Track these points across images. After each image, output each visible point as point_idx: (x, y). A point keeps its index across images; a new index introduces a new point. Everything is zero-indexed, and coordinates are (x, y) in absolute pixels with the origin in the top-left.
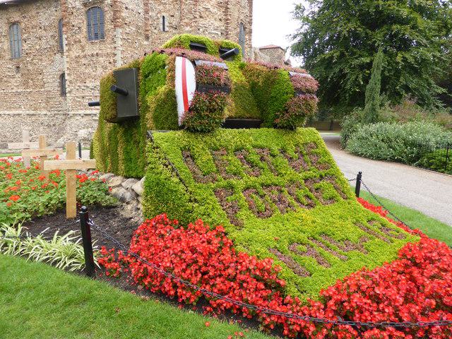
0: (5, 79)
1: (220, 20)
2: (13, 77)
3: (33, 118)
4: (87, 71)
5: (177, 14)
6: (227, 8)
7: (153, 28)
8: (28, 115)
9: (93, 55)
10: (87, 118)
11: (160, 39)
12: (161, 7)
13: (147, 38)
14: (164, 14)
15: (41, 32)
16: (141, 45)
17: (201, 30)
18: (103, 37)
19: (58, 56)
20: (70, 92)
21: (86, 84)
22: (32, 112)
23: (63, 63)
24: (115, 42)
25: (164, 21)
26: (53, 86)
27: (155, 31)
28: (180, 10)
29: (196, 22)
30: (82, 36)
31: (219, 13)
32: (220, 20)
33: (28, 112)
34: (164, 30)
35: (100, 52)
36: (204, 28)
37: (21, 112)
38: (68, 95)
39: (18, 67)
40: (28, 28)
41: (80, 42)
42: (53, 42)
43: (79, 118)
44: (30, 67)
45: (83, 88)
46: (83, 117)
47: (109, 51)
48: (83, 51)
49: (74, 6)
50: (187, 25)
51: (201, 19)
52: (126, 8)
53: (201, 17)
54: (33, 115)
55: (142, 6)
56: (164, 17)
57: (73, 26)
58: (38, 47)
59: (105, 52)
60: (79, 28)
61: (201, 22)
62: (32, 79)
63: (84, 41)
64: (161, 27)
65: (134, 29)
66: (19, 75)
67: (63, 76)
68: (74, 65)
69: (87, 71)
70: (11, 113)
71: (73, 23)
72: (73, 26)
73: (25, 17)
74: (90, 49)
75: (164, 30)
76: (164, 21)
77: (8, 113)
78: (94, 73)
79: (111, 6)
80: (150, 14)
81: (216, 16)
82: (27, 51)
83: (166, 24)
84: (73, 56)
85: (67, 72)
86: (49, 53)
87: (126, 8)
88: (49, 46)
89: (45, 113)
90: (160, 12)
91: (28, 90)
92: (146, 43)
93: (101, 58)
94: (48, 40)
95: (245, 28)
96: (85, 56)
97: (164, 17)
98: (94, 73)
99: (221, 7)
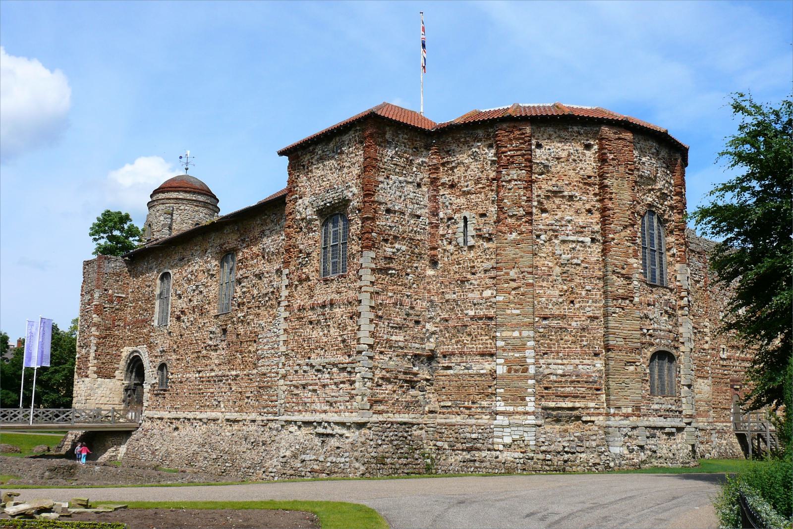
0: (204, 352)
1: (589, 211)
3: (236, 427)
4: (314, 334)
6: (603, 187)
7: (445, 243)
8: (228, 420)
9: (324, 306)
10: (305, 430)
11: (459, 264)
12: (462, 200)
13: (434, 263)
14: (466, 213)
15: (263, 266)
16: (420, 277)
17: (543, 237)
20: (284, 377)
21: (311, 361)
24: (360, 278)
25: (466, 226)
27: (451, 248)
28: (499, 201)
29: (530, 222)
32: (589, 211)
33: (228, 416)
34: (465, 242)
35: (337, 297)
36: (551, 233)
37: (218, 415)
39: (225, 331)
40: (246, 259)
41: (308, 279)
43: (293, 428)
44: (241, 331)
45: (305, 368)
46: (300, 427)
47: (351, 294)
48: (311, 297)
49: (304, 216)
51: (544, 215)
52: (388, 211)
53: (544, 211)
54: (236, 421)
55: (425, 201)
56: (465, 219)
57: (301, 252)
58: (255, 292)
60: (308, 255)
62: (241, 352)
63: (314, 276)
65: (404, 248)
66: (224, 344)
68: (296, 323)
69: (314, 334)
70: (203, 416)
71: (301, 247)
72: (301, 252)
73: (243, 241)
75: (465, 242)
76: (466, 226)
78: (325, 339)
79: (359, 210)
80: (441, 215)
81: (578, 205)
82: (240, 300)
83: (471, 231)
84: (296, 306)
86: (269, 303)
87: (388, 211)
88: (272, 290)
90: (459, 210)
91: (234, 373)
92: (430, 272)
93: (337, 310)
95: (662, 222)
96: (313, 309)
97: (465, 219)
98: (325, 339)
99: (589, 185)
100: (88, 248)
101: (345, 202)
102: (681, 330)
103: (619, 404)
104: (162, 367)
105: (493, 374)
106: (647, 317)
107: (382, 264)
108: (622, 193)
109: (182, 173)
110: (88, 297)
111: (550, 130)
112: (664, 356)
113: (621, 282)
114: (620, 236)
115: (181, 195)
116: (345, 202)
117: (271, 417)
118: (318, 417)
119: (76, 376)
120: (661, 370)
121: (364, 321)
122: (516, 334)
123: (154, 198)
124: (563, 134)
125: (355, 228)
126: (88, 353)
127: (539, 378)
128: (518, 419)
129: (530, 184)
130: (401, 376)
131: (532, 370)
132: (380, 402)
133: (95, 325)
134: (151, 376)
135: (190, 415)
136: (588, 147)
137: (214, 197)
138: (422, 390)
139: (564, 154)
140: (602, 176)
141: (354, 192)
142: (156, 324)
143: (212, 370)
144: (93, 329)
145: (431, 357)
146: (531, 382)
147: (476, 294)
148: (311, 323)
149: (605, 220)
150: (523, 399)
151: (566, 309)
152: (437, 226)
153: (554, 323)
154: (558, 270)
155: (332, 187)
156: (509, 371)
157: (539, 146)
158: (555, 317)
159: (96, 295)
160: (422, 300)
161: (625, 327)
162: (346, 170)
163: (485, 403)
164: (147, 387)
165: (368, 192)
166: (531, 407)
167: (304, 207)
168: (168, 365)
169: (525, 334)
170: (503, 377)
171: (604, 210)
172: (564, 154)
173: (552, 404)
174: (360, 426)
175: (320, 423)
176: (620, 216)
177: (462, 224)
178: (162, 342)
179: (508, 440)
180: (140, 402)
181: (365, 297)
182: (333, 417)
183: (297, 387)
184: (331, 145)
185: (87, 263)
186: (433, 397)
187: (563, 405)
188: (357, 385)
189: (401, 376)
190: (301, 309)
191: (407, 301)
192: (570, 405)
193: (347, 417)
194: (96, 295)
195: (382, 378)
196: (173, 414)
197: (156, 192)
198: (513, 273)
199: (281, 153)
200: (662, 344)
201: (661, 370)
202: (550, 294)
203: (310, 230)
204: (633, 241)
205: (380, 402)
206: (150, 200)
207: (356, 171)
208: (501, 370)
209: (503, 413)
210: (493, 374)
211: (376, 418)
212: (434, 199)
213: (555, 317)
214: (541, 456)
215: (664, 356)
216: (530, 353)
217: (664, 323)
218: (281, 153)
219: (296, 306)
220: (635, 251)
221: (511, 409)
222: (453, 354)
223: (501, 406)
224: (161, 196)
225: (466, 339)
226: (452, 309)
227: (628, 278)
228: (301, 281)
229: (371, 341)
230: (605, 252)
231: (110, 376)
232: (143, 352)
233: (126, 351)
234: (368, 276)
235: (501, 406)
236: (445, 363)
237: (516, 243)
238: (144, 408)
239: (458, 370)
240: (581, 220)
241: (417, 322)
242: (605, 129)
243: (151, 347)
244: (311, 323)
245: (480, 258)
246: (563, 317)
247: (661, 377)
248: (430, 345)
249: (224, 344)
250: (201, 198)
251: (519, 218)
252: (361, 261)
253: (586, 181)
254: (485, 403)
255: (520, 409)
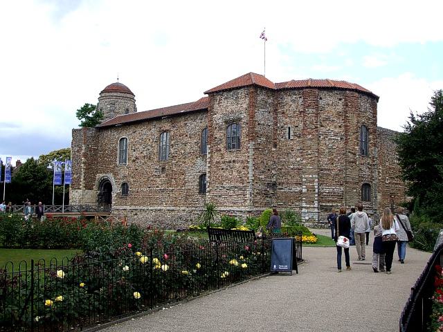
2: (159, 177)
5: (301, 125)
9: (230, 162)
12: (288, 120)
13: (275, 146)
15: (186, 139)
16: (270, 151)
18: (239, 147)
19: (199, 161)
20: (209, 192)
22: (172, 208)
23: (201, 166)
26: (194, 185)
30: (222, 146)
31: (340, 122)
32: (340, 127)
33: (168, 208)
38: (207, 194)
41: (220, 150)
42: (196, 148)
47: (243, 158)
49: (218, 122)
50: (309, 134)
52: (259, 124)
54: (173, 210)
56: (289, 128)
58: (183, 152)
59: (240, 159)
61: (323, 129)
64: (287, 137)
66: (164, 175)
67: (203, 177)
74: (229, 157)
77: (152, 208)
83: (292, 133)
84: (215, 161)
85: (208, 175)
89: (183, 208)
92: (274, 149)
94: (192, 145)
97: (289, 128)
100: (77, 123)
101: (240, 119)
102: (373, 174)
103: (350, 204)
104: (124, 184)
105: (301, 192)
106: (361, 169)
107: (257, 146)
108: (354, 120)
109: (115, 81)
110: (77, 149)
111: (325, 92)
112: (367, 186)
113: (351, 156)
114: (352, 137)
115: (119, 94)
116: (240, 119)
117: (193, 209)
118: (228, 209)
119: (70, 189)
120: (365, 191)
121: (250, 170)
122: (311, 176)
123: (103, 95)
124: (330, 94)
125: (245, 131)
126: (80, 177)
127: (319, 194)
128: (311, 210)
129: (317, 115)
130: (263, 192)
131: (317, 191)
132: (257, 202)
133: (84, 163)
134: (116, 190)
135: (145, 208)
136: (340, 99)
137: (133, 94)
138: (270, 197)
139: (331, 103)
140: (346, 112)
141: (244, 116)
142: (118, 163)
143: (157, 187)
144: (82, 165)
145: (274, 184)
146: (316, 195)
147: (294, 159)
148: (223, 169)
149: (346, 131)
150: (313, 202)
151: (330, 167)
152: (277, 130)
153: (325, 172)
154: (327, 151)
155: (232, 111)
156: (308, 190)
157: (321, 99)
158: (325, 170)
159: (83, 148)
160: (271, 161)
161: (353, 174)
162: (239, 106)
163: (297, 204)
164: (114, 195)
165: (252, 117)
166: (316, 205)
167: (218, 118)
168: (128, 184)
169: (314, 176)
170: (305, 193)
171: (346, 126)
172: (331, 103)
173: (324, 204)
174: (249, 212)
175: (229, 211)
176: (352, 129)
177: (288, 130)
178: (123, 172)
179: (307, 218)
180: (111, 203)
181: (250, 160)
182: (235, 208)
183: (216, 196)
184: (231, 93)
185: (74, 131)
186: (274, 201)
187: (328, 204)
188: (247, 196)
189: (263, 192)
190: (217, 162)
191: (265, 161)
192: (331, 204)
193: (243, 209)
194: (83, 148)
195: (257, 193)
196: (133, 207)
197: (102, 92)
198: (309, 152)
199: (205, 93)
200: (366, 181)
201: (365, 191)
202: (324, 160)
203: (221, 129)
204: (357, 139)
205: (257, 202)
206: (99, 96)
207: (245, 106)
208: (304, 191)
209: (305, 207)
210: (301, 192)
211: (255, 209)
212: (275, 118)
213: (325, 170)
214: (320, 225)
215: (367, 186)
216: (316, 184)
217: (367, 172)
218: (205, 93)
219: (215, 161)
220: (358, 143)
221: (308, 206)
222: (283, 183)
223: (304, 205)
224: (107, 94)
225: (289, 178)
226: (283, 165)
227: (355, 154)
228: (217, 150)
229: (253, 178)
230: (346, 143)
231: (91, 189)
232: (111, 177)
233: (99, 176)
234: (252, 152)
235: (304, 205)
236: (280, 187)
237: (311, 139)
238: (112, 205)
239: (286, 190)
240: (337, 130)
241: (269, 170)
242: (347, 92)
243: (115, 174)
244: (223, 169)
245: (295, 144)
246: (329, 170)
247: (365, 194)
248: (274, 180)
249: (164, 175)
250: (128, 95)
251: (312, 129)
252: (249, 145)
253: (339, 114)
254: (297, 204)
255: (312, 206)
